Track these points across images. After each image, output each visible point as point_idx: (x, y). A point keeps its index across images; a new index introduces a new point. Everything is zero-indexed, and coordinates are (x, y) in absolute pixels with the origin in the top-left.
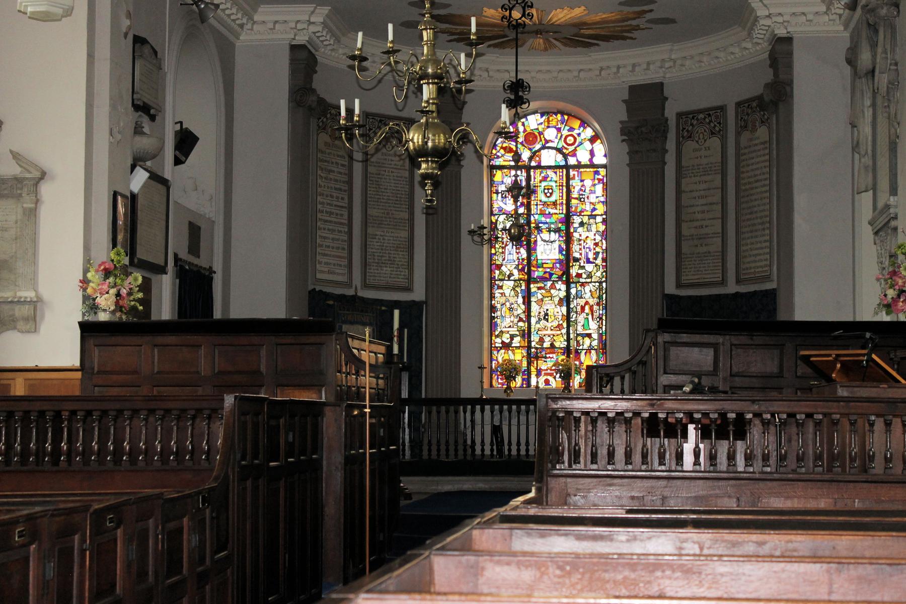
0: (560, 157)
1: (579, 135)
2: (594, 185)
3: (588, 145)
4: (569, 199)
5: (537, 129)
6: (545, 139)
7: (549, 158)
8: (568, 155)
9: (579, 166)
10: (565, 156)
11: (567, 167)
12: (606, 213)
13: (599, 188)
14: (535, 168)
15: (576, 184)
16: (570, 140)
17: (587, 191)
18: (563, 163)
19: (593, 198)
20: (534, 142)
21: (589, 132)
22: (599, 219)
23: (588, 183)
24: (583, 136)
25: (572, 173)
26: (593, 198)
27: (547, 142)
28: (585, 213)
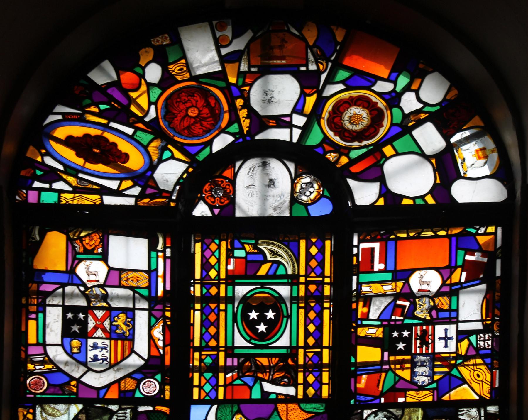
0: (311, 189)
1: (393, 99)
2: (451, 291)
3: (430, 138)
5: (221, 75)
6: (252, 114)
7: (262, 190)
8: (346, 172)
9: (395, 217)
10: (335, 185)
12: (498, 395)
13: (471, 306)
14: (208, 229)
17: (422, 312)
18: (323, 208)
19: (444, 340)
20: (211, 123)
21: (433, 91)
23: (427, 281)
24: (409, 103)
25: (360, 246)
26: (444, 340)
27: (261, 122)
28: (412, 396)
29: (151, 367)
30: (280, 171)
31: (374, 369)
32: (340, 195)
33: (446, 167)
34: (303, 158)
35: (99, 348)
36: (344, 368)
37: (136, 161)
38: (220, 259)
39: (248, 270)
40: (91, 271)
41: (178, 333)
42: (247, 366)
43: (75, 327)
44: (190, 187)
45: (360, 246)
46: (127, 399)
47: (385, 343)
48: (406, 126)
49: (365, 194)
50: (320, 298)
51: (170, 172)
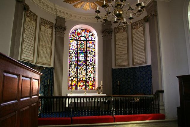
0: (85, 39)
3: (91, 36)
4: (87, 47)
7: (82, 38)
9: (89, 40)
10: (86, 38)
11: (87, 41)
14: (79, 40)
15: (88, 45)
16: (87, 35)
20: (79, 35)
22: (93, 52)
23: (91, 44)
24: (90, 34)
25: (87, 42)
26: (92, 48)
27: (82, 35)
29: (76, 48)
30: (83, 37)
31: (88, 49)
32: (86, 39)
33: (92, 38)
34: (85, 37)
35: (74, 47)
36: (87, 49)
37: (76, 37)
38: (80, 42)
39: (81, 43)
40: (73, 42)
41: (78, 46)
42: (81, 48)
43: (72, 46)
44: (78, 38)
45: (87, 42)
46: (75, 50)
47: (89, 48)
48: (89, 36)
49: (88, 39)
50: (85, 45)
51: (78, 37)
